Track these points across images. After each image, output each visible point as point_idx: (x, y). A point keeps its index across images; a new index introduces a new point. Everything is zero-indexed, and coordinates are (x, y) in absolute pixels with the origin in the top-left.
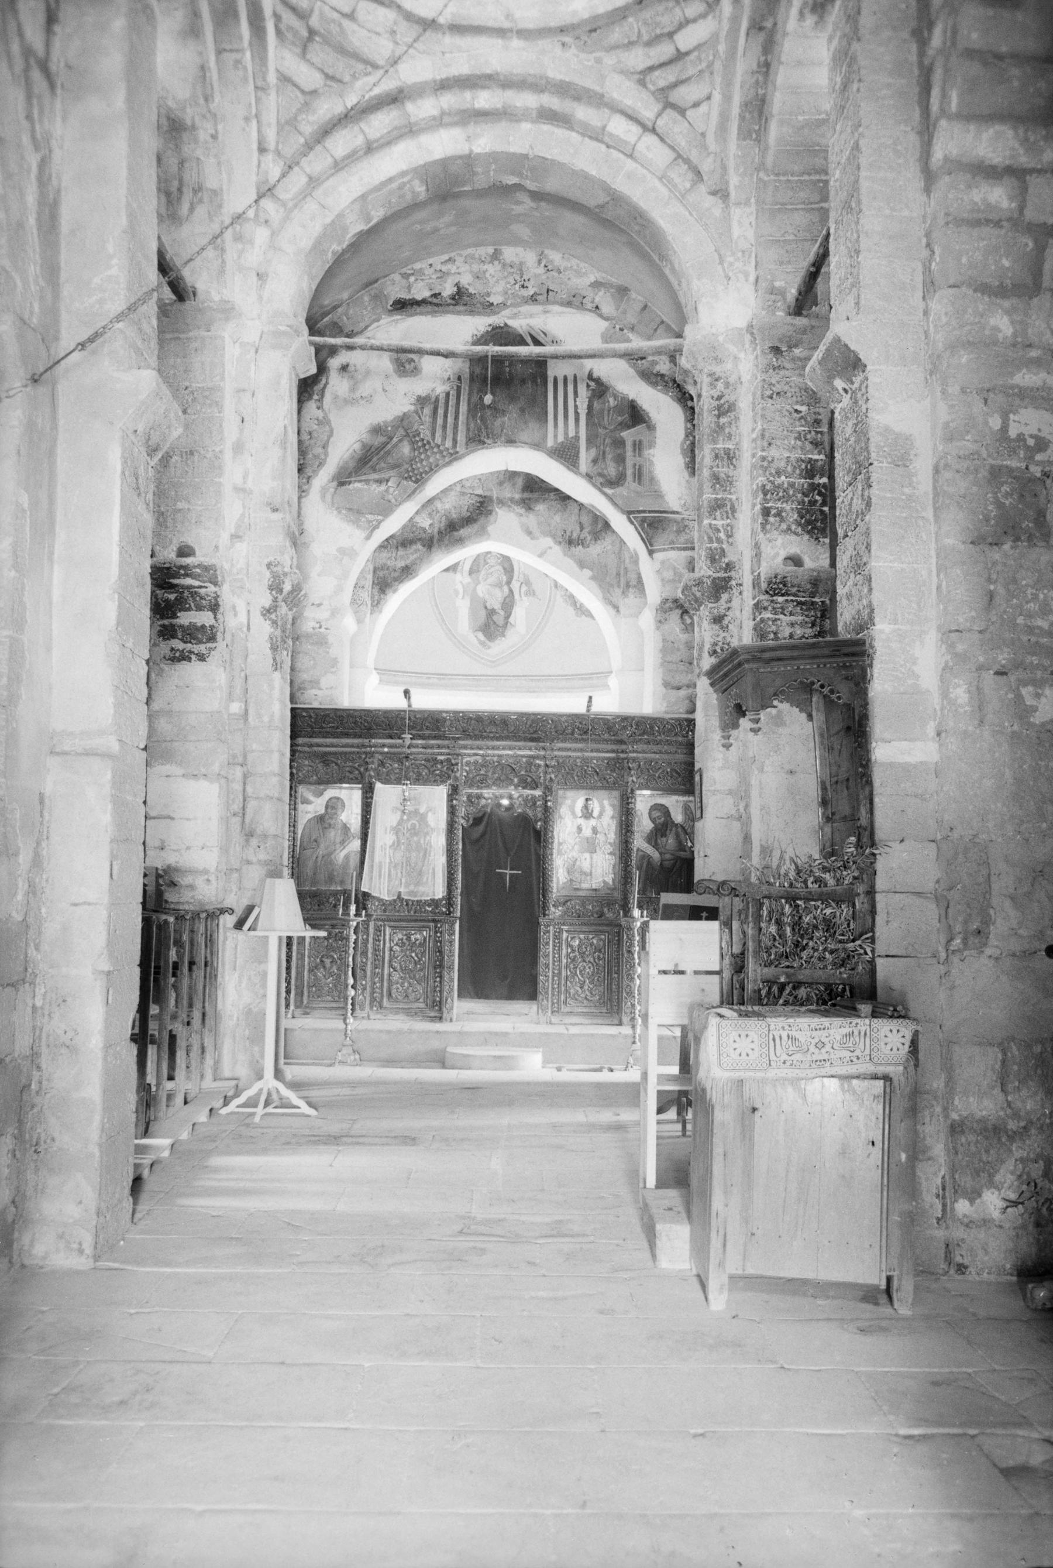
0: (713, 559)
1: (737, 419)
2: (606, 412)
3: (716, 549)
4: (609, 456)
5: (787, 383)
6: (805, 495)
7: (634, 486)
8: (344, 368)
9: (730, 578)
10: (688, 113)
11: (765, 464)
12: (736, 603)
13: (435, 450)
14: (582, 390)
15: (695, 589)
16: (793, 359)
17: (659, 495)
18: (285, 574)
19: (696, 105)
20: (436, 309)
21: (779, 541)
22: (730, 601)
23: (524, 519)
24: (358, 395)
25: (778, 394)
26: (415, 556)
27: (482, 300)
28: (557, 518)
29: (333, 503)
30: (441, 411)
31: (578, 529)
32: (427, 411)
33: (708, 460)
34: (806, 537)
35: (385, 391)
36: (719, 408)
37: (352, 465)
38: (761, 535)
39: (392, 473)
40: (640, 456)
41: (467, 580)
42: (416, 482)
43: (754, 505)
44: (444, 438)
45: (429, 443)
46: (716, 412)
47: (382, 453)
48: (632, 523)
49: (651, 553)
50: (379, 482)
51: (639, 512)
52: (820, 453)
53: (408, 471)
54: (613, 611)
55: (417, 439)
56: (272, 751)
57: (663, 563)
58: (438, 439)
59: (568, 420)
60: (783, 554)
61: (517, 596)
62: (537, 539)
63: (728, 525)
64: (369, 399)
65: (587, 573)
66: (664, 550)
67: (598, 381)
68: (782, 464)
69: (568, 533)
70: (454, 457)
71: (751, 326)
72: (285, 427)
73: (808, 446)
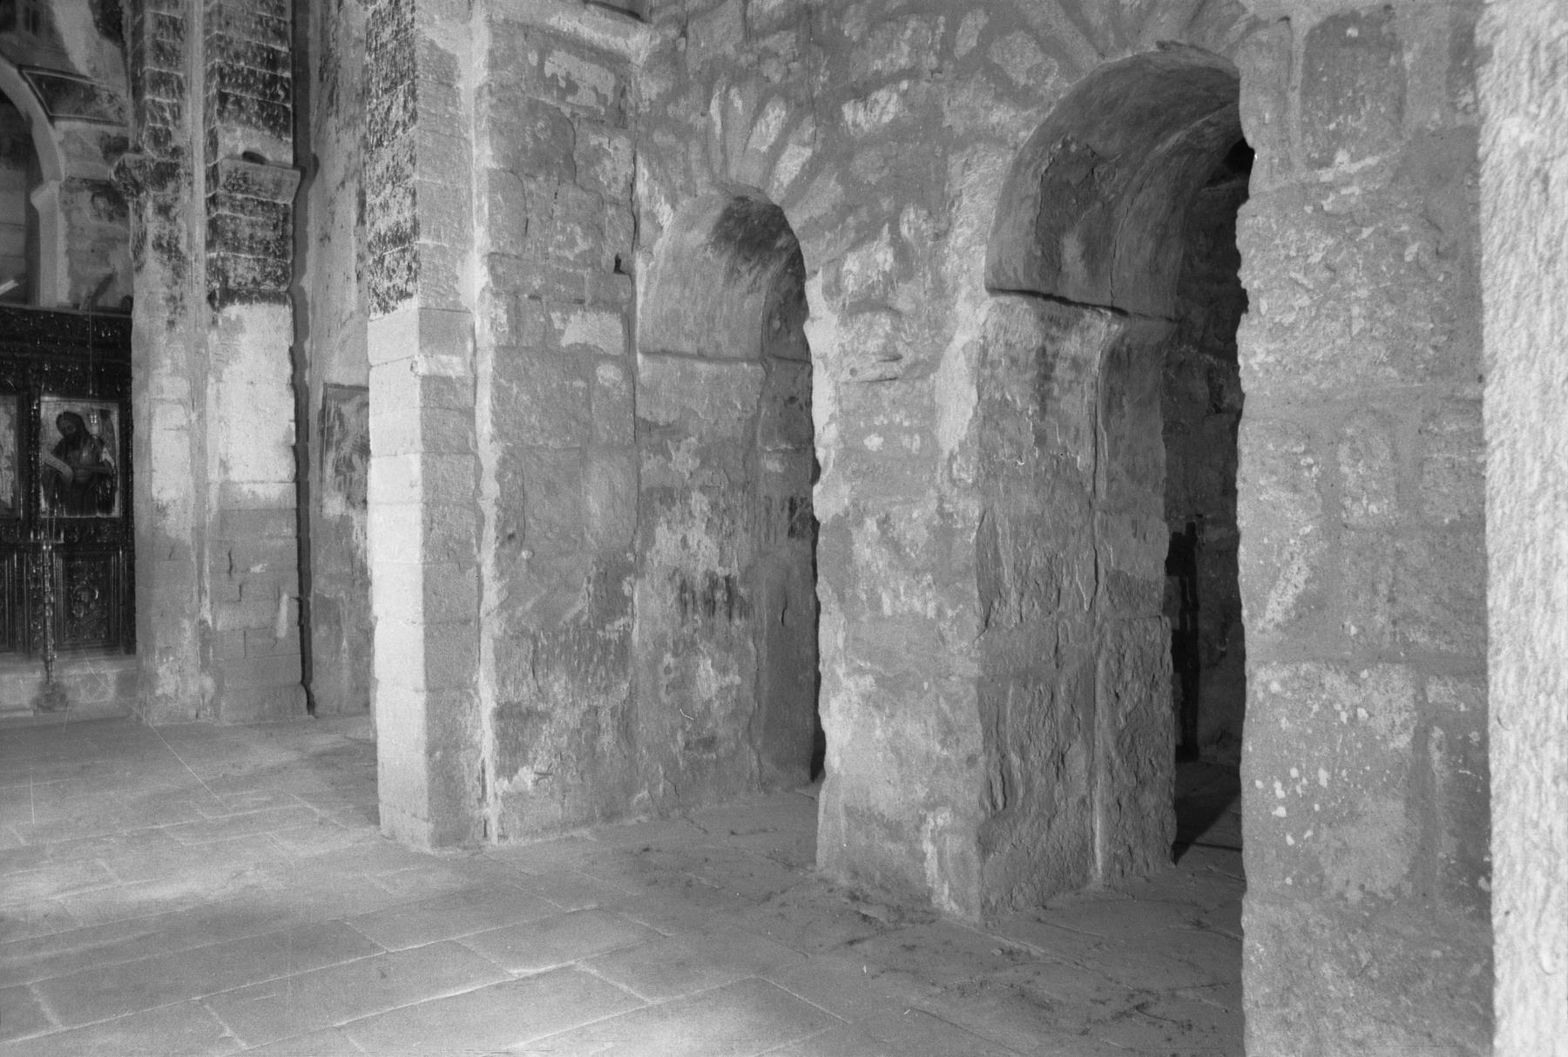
12: (185, 196)
17: (60, 52)
21: (239, 133)
22: (177, 190)
34: (267, 133)
38: (218, 123)
43: (207, 89)
48: (25, 79)
49: (52, 119)
51: (37, 68)
52: (282, 44)
57: (68, 134)
66: (69, 119)
68: (242, 48)
73: (270, 34)
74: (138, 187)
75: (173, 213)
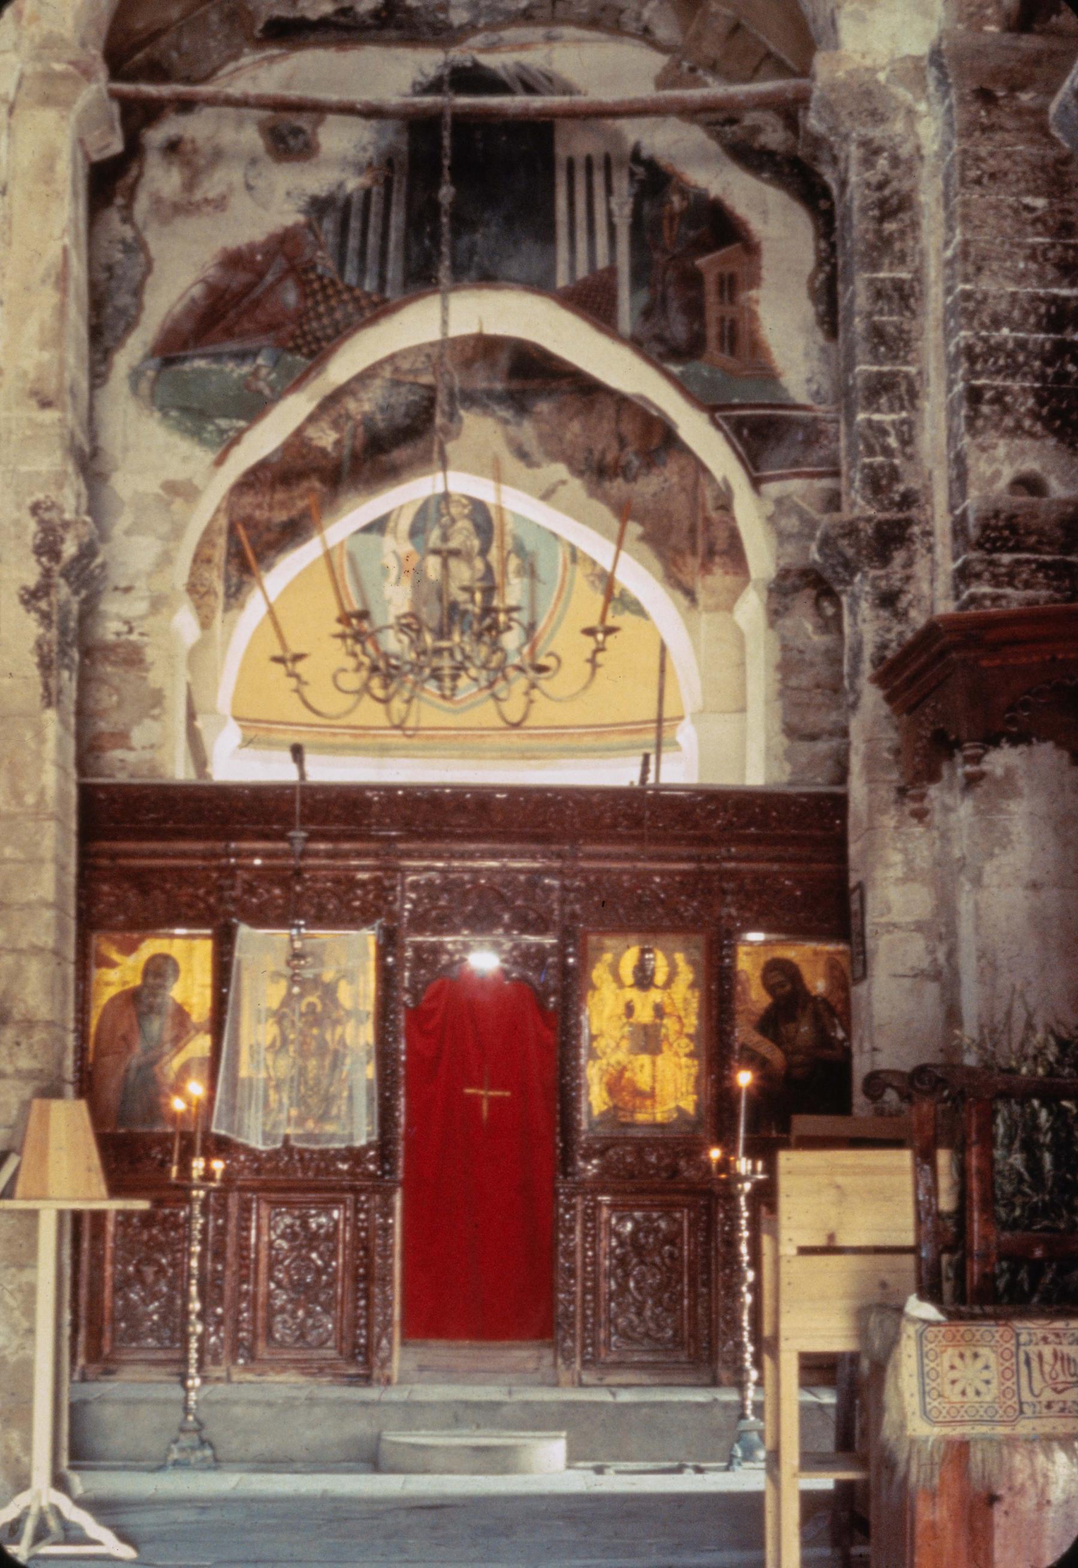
0: (878, 483)
1: (915, 225)
2: (666, 222)
3: (881, 467)
4: (674, 305)
5: (1009, 156)
6: (1047, 362)
7: (724, 357)
8: (173, 147)
9: (909, 522)
11: (971, 306)
12: (921, 568)
13: (346, 296)
14: (622, 185)
15: (843, 543)
16: (1019, 113)
17: (769, 376)
18: (66, 525)
20: (346, 36)
21: (1001, 451)
22: (909, 563)
23: (512, 430)
24: (198, 195)
25: (992, 176)
26: (306, 502)
27: (430, 18)
28: (576, 426)
29: (153, 395)
30: (355, 224)
31: (615, 446)
32: (329, 224)
33: (862, 301)
34: (1051, 442)
35: (249, 187)
36: (882, 203)
37: (188, 326)
38: (967, 439)
39: (263, 340)
40: (732, 301)
41: (407, 547)
42: (311, 354)
43: (951, 383)
44: (362, 271)
45: (333, 283)
46: (876, 213)
47: (245, 303)
49: (756, 483)
50: (242, 356)
53: (293, 337)
54: (684, 602)
55: (312, 276)
56: (42, 861)
57: (779, 502)
58: (351, 276)
59: (595, 232)
60: (1008, 473)
62: (538, 465)
63: (903, 422)
64: (220, 204)
65: (634, 529)
68: (1003, 306)
69: (597, 455)
70: (379, 309)
71: (936, 56)
72: (65, 250)
73: (1051, 273)
74: (850, 567)
75: (903, 603)
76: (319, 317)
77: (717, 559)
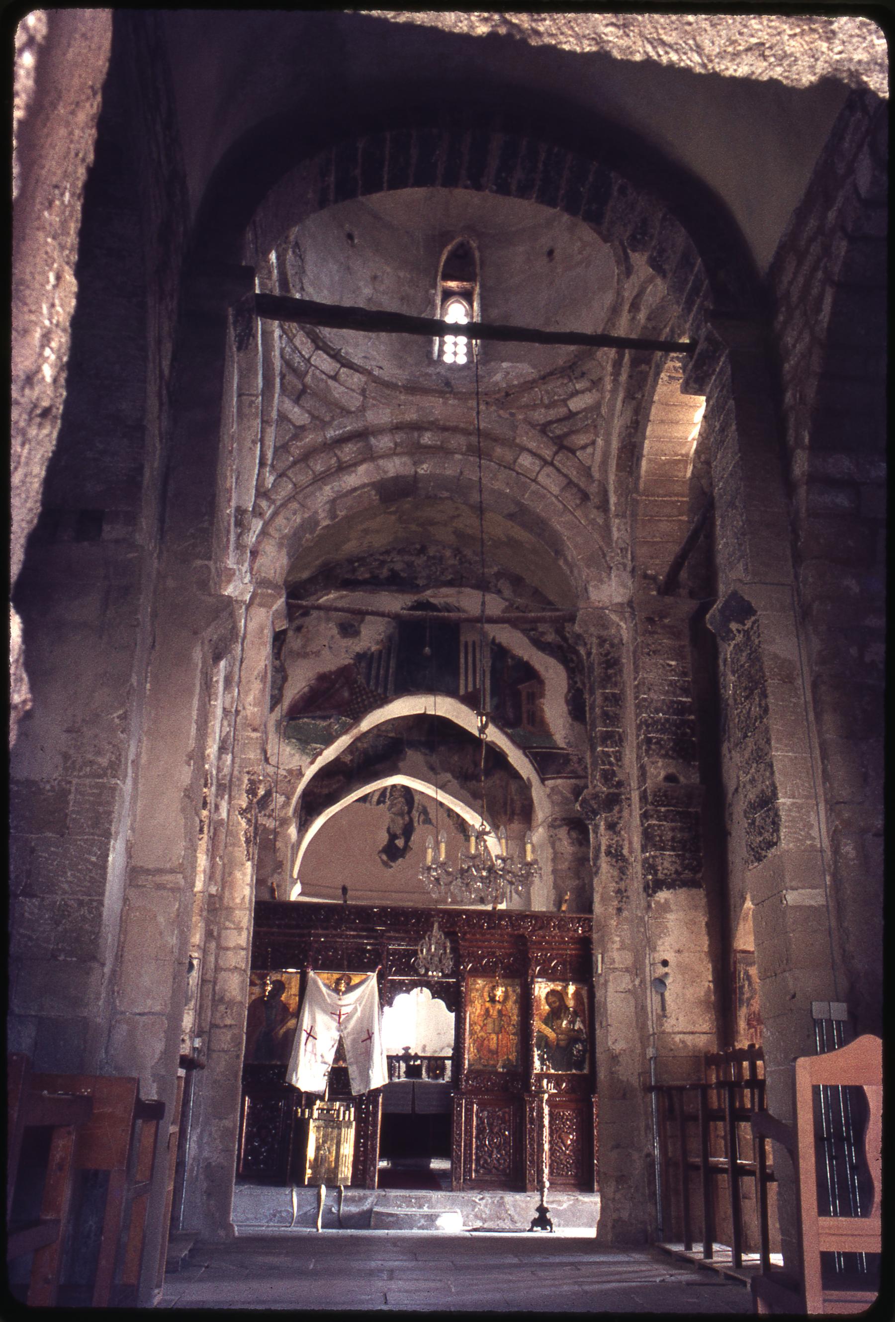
0: (608, 777)
1: (621, 671)
3: (608, 770)
5: (660, 644)
6: (678, 728)
9: (620, 794)
10: (578, 453)
11: (646, 704)
12: (625, 813)
13: (370, 695)
14: (487, 653)
15: (593, 802)
16: (664, 627)
17: (548, 735)
18: (260, 781)
19: (584, 448)
21: (660, 764)
22: (620, 811)
25: (654, 652)
29: (285, 733)
32: (363, 664)
33: (599, 701)
36: (607, 662)
43: (638, 736)
44: (377, 684)
45: (364, 689)
46: (604, 666)
49: (543, 781)
50: (324, 718)
52: (687, 697)
56: (242, 928)
57: (552, 789)
59: (477, 672)
60: (663, 774)
61: (416, 824)
63: (617, 752)
67: (500, 646)
71: (630, 603)
72: (266, 666)
73: (678, 692)
74: (595, 813)
75: (618, 829)
76: (358, 703)
77: (516, 817)
